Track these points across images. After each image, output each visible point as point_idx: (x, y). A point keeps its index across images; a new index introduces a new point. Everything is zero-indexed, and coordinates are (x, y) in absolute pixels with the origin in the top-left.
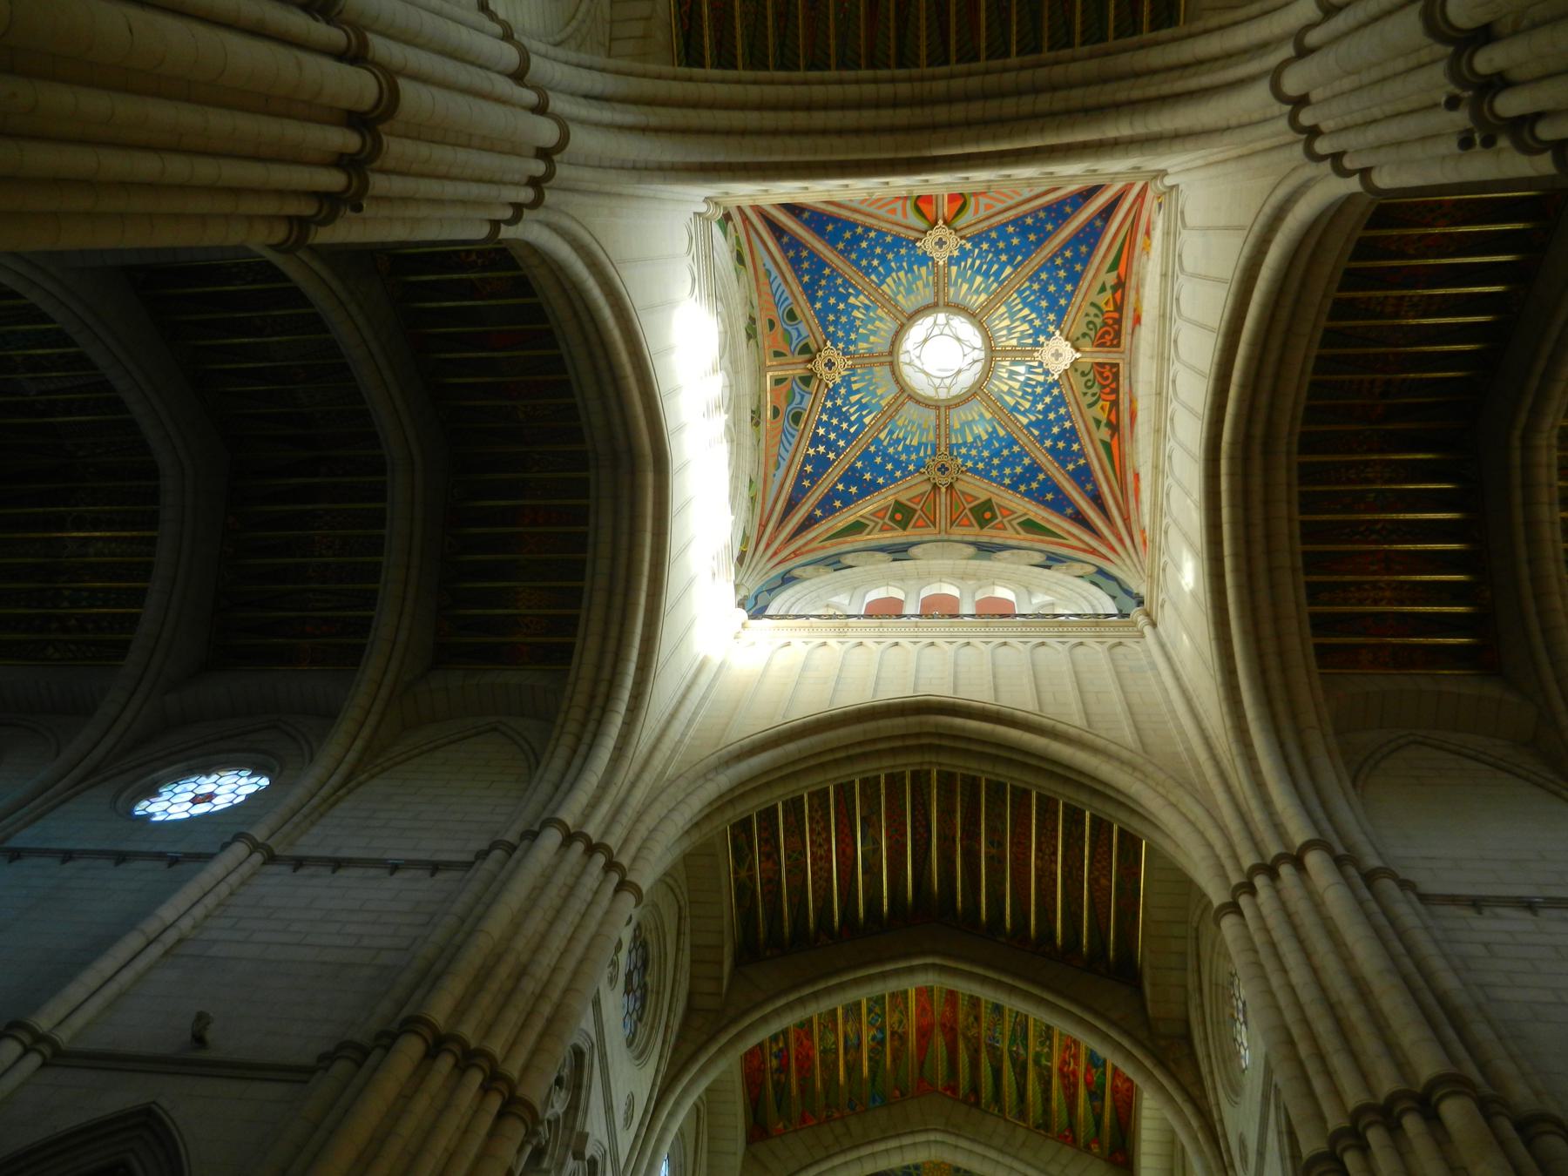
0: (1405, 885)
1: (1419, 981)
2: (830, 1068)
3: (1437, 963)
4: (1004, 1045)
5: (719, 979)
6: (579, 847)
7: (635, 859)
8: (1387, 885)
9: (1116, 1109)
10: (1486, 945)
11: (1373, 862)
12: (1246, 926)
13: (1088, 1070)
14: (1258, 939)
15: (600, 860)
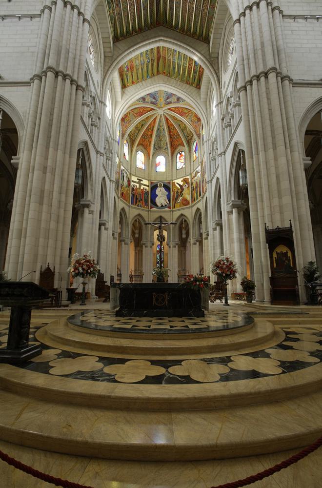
0: (281, 12)
1: (275, 43)
2: (137, 70)
3: (280, 37)
4: (176, 61)
5: (110, 47)
6: (69, 7)
7: (85, 10)
8: (277, 12)
9: (199, 75)
10: (292, 31)
11: (275, 4)
12: (240, 26)
13: (194, 66)
14: (243, 30)
15: (76, 11)
